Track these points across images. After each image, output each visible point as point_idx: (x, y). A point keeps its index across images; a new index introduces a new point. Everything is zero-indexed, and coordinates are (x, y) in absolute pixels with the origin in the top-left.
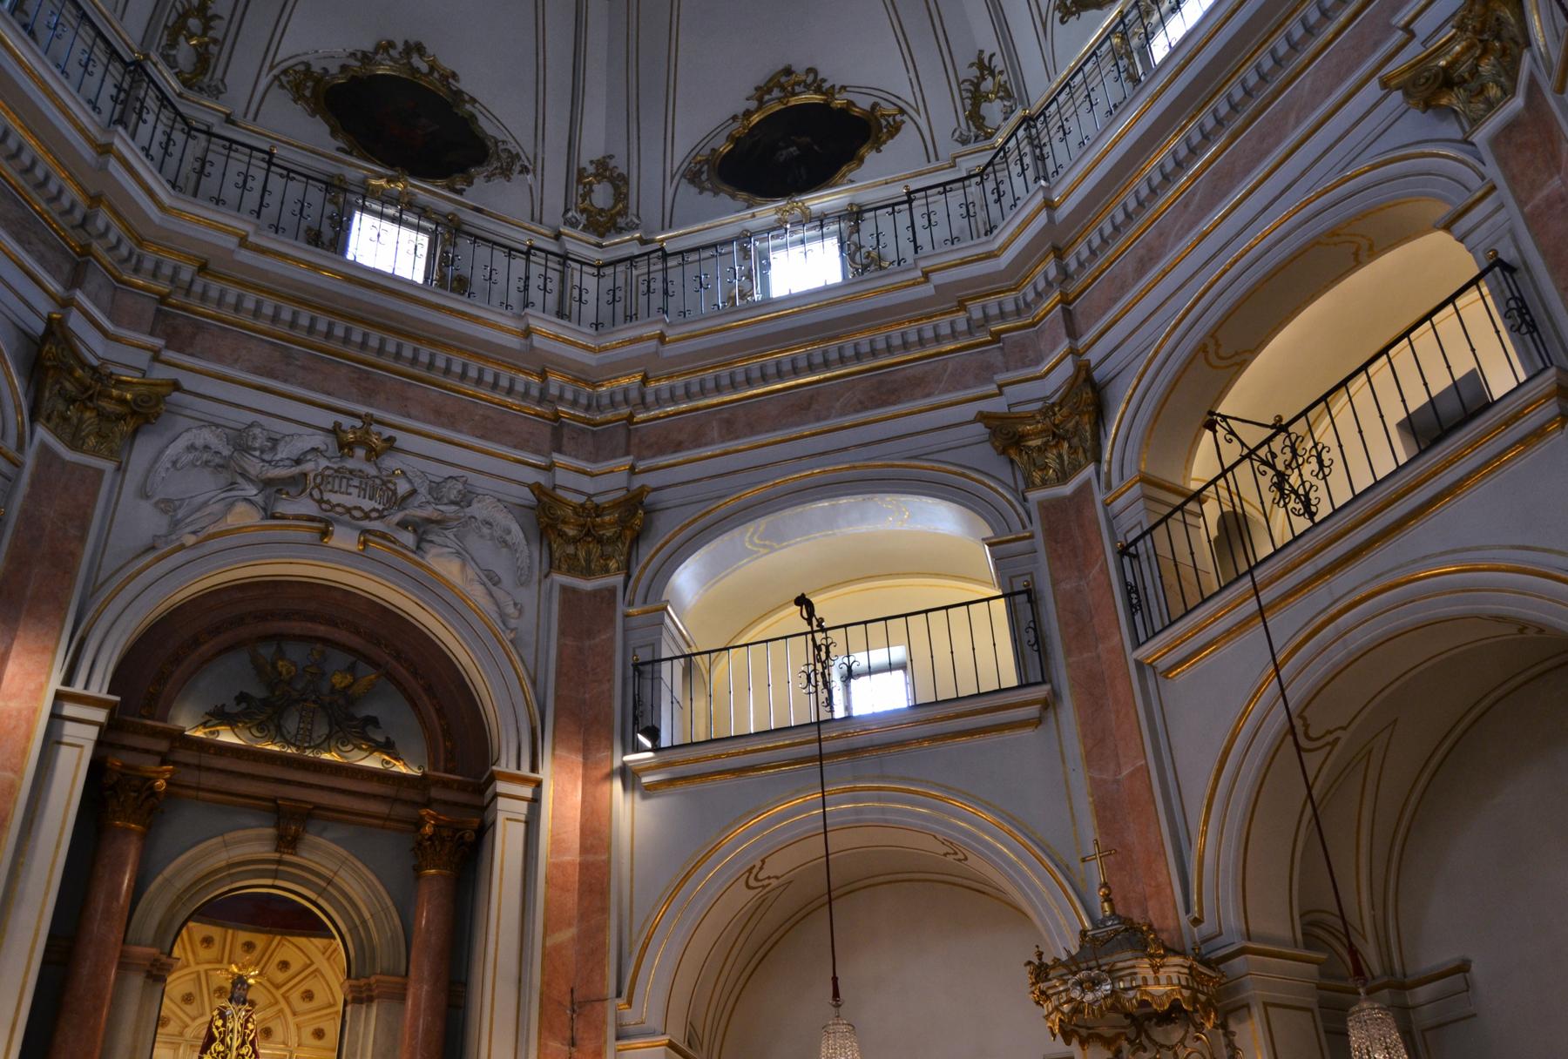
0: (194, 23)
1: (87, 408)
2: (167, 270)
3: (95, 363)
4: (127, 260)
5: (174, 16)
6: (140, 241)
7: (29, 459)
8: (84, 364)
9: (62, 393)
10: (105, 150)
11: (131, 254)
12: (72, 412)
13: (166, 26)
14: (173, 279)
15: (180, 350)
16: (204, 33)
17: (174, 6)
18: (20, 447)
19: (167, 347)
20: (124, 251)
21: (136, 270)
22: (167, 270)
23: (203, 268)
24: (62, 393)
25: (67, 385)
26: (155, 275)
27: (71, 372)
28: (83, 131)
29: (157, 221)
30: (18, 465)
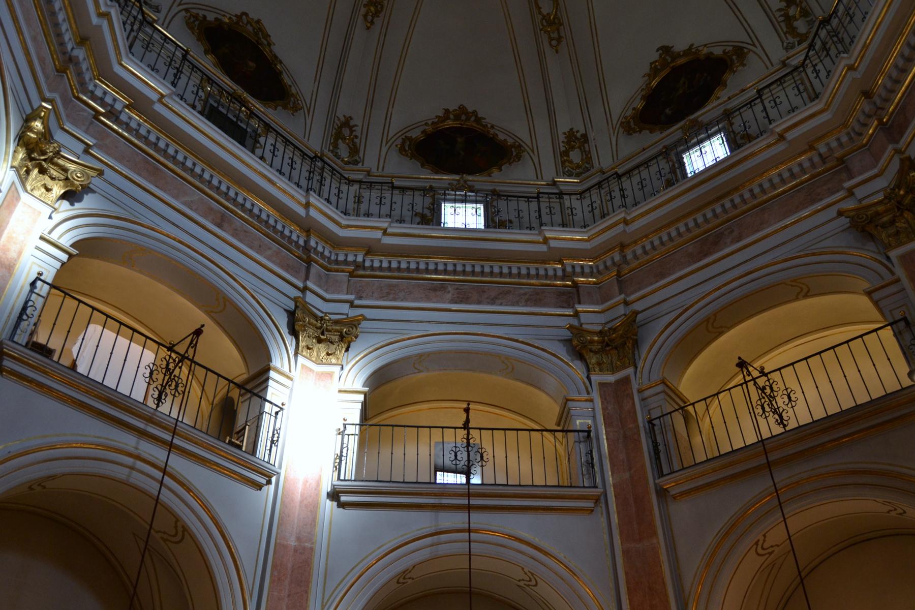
0: (792, 11)
1: (901, 215)
2: (862, 119)
3: (880, 197)
4: (851, 139)
5: (783, 25)
6: (845, 125)
7: (900, 272)
8: (880, 203)
9: (884, 226)
10: (782, 137)
11: (848, 134)
12: (900, 224)
13: (785, 34)
14: (869, 116)
15: (902, 134)
16: (797, 6)
17: (778, 23)
18: (893, 273)
19: (897, 142)
20: (844, 139)
21: (860, 134)
22: (862, 118)
23: (867, 95)
24: (884, 226)
25: (885, 219)
26: (865, 125)
27: (878, 214)
28: (769, 146)
29: (830, 116)
30: (898, 280)
